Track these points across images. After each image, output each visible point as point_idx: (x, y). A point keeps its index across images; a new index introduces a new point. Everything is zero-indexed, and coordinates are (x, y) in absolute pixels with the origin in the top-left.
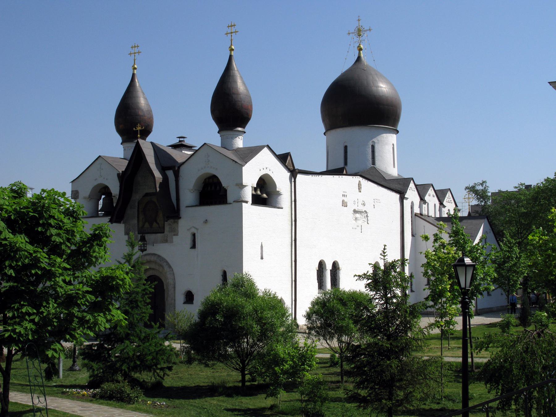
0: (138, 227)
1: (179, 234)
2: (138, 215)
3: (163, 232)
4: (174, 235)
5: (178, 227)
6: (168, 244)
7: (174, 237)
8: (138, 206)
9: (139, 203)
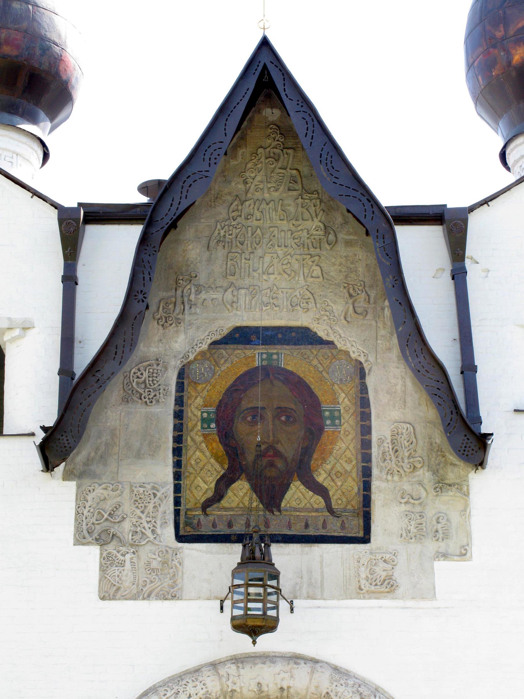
0: (177, 502)
1: (475, 550)
2: (178, 439)
3: (365, 539)
4: (445, 556)
5: (465, 511)
6: (399, 603)
7: (440, 565)
8: (180, 387)
9: (181, 375)
